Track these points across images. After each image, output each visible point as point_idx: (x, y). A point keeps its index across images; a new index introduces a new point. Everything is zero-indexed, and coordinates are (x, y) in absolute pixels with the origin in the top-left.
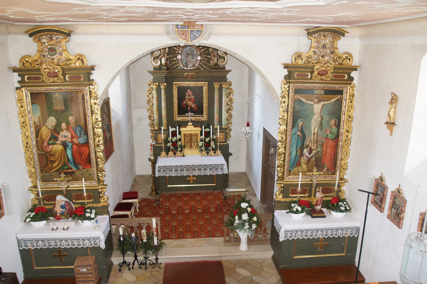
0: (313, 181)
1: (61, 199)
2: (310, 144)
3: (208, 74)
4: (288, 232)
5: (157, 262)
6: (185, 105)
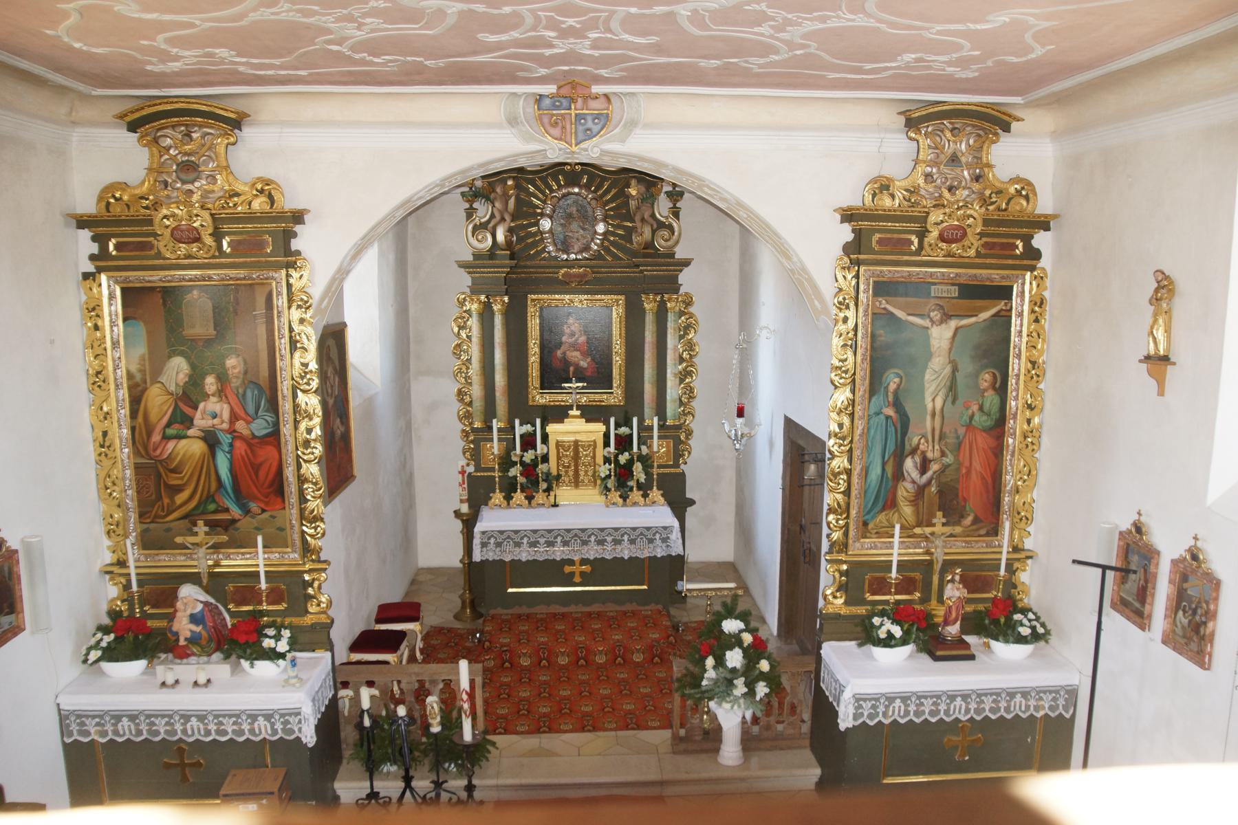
0: (931, 554)
1: (191, 596)
2: (923, 444)
3: (626, 273)
4: (865, 700)
5: (470, 796)
6: (561, 361)
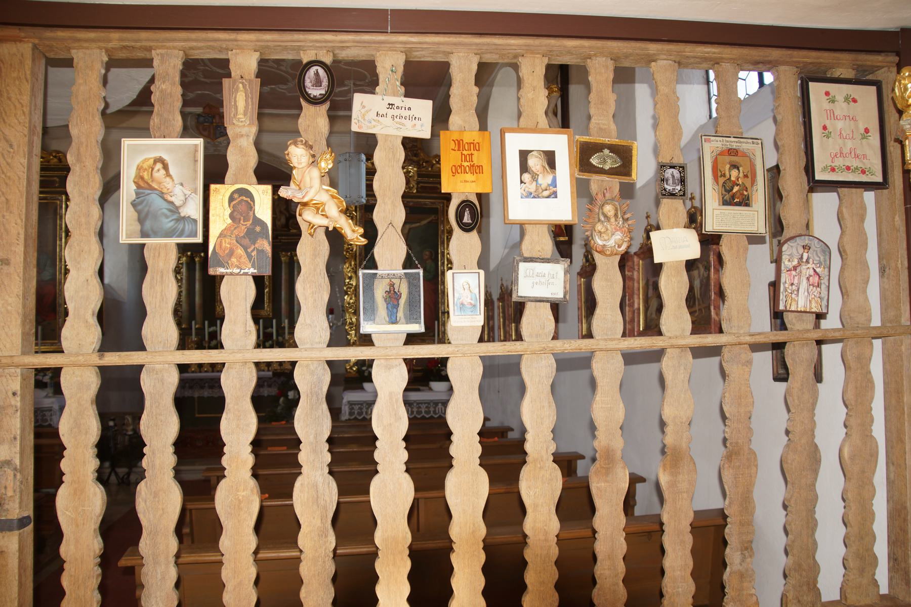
4: (355, 404)
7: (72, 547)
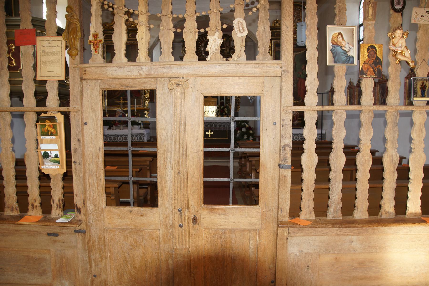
7: (307, 176)
